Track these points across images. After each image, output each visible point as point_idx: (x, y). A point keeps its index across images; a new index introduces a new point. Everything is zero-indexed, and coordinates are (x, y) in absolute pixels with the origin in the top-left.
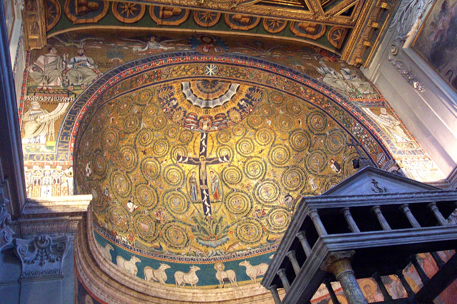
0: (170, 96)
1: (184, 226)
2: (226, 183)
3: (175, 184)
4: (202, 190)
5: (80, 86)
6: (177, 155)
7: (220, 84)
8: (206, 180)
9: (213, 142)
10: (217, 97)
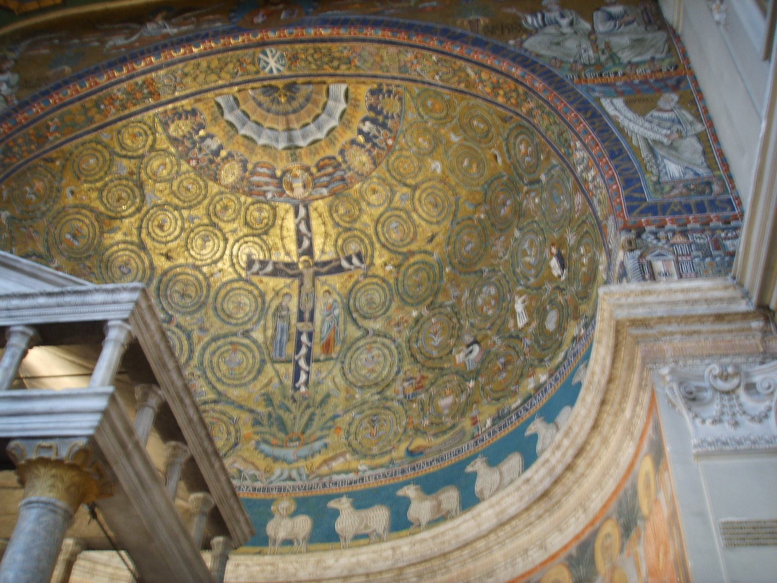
0: (197, 133)
1: (235, 413)
2: (355, 315)
3: (240, 321)
4: (299, 334)
6: (244, 258)
7: (305, 90)
9: (324, 223)
10: (309, 120)
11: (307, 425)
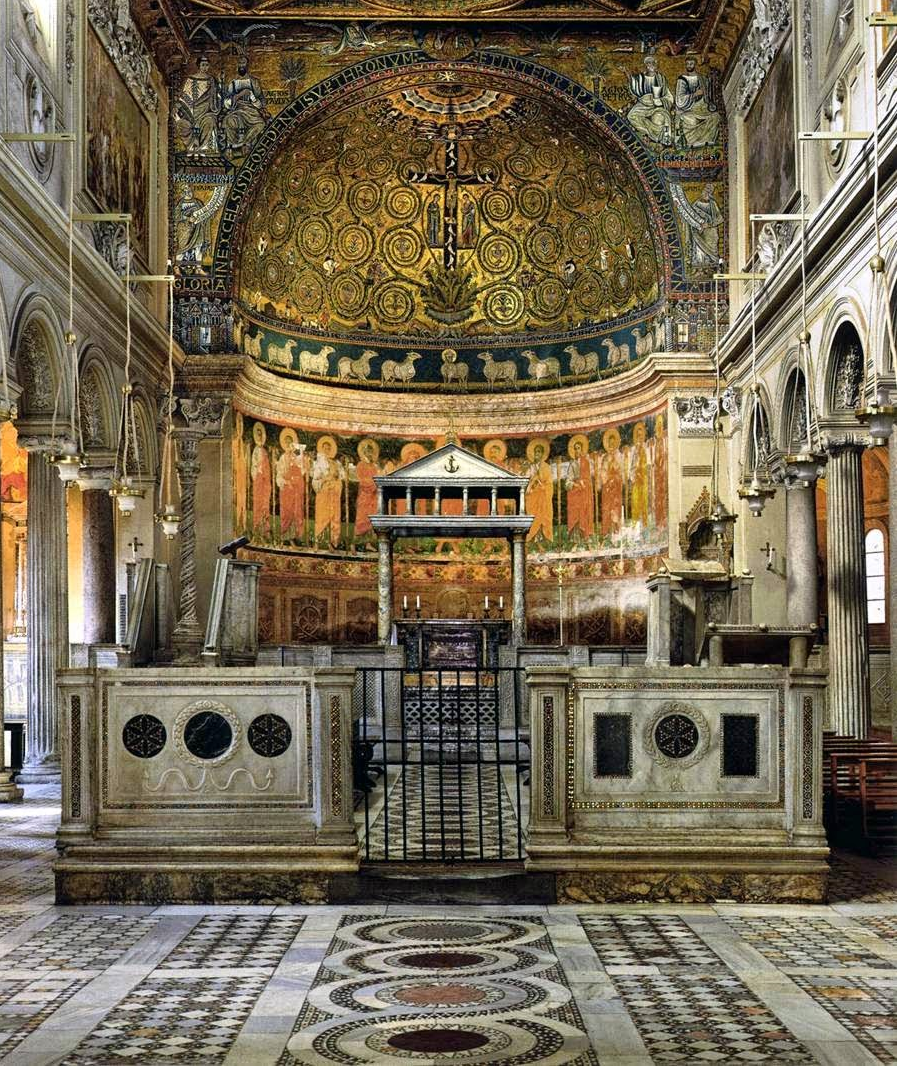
1: (409, 287)
4: (446, 225)
5: (239, 149)
8: (455, 210)
11: (458, 297)
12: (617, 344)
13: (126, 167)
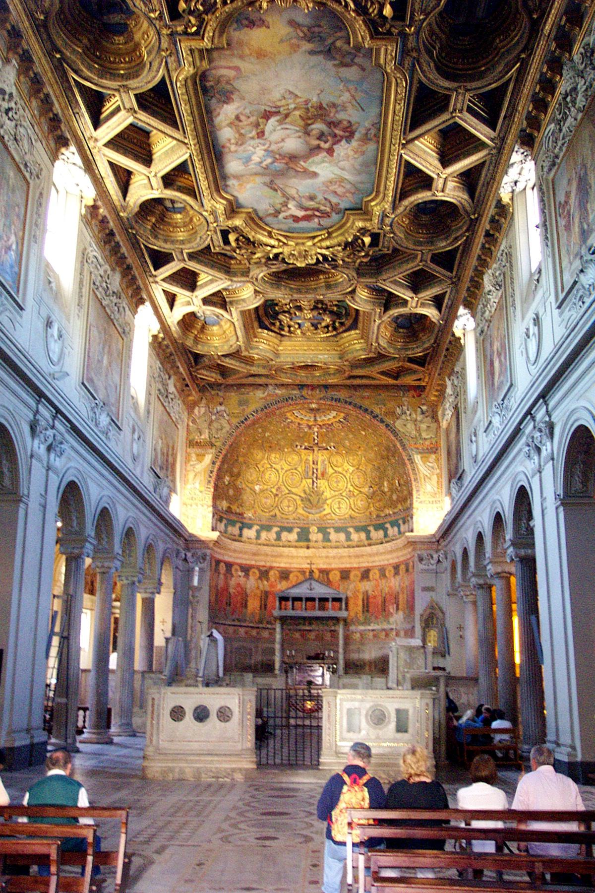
1: (295, 497)
12: (392, 527)
13: (168, 451)
